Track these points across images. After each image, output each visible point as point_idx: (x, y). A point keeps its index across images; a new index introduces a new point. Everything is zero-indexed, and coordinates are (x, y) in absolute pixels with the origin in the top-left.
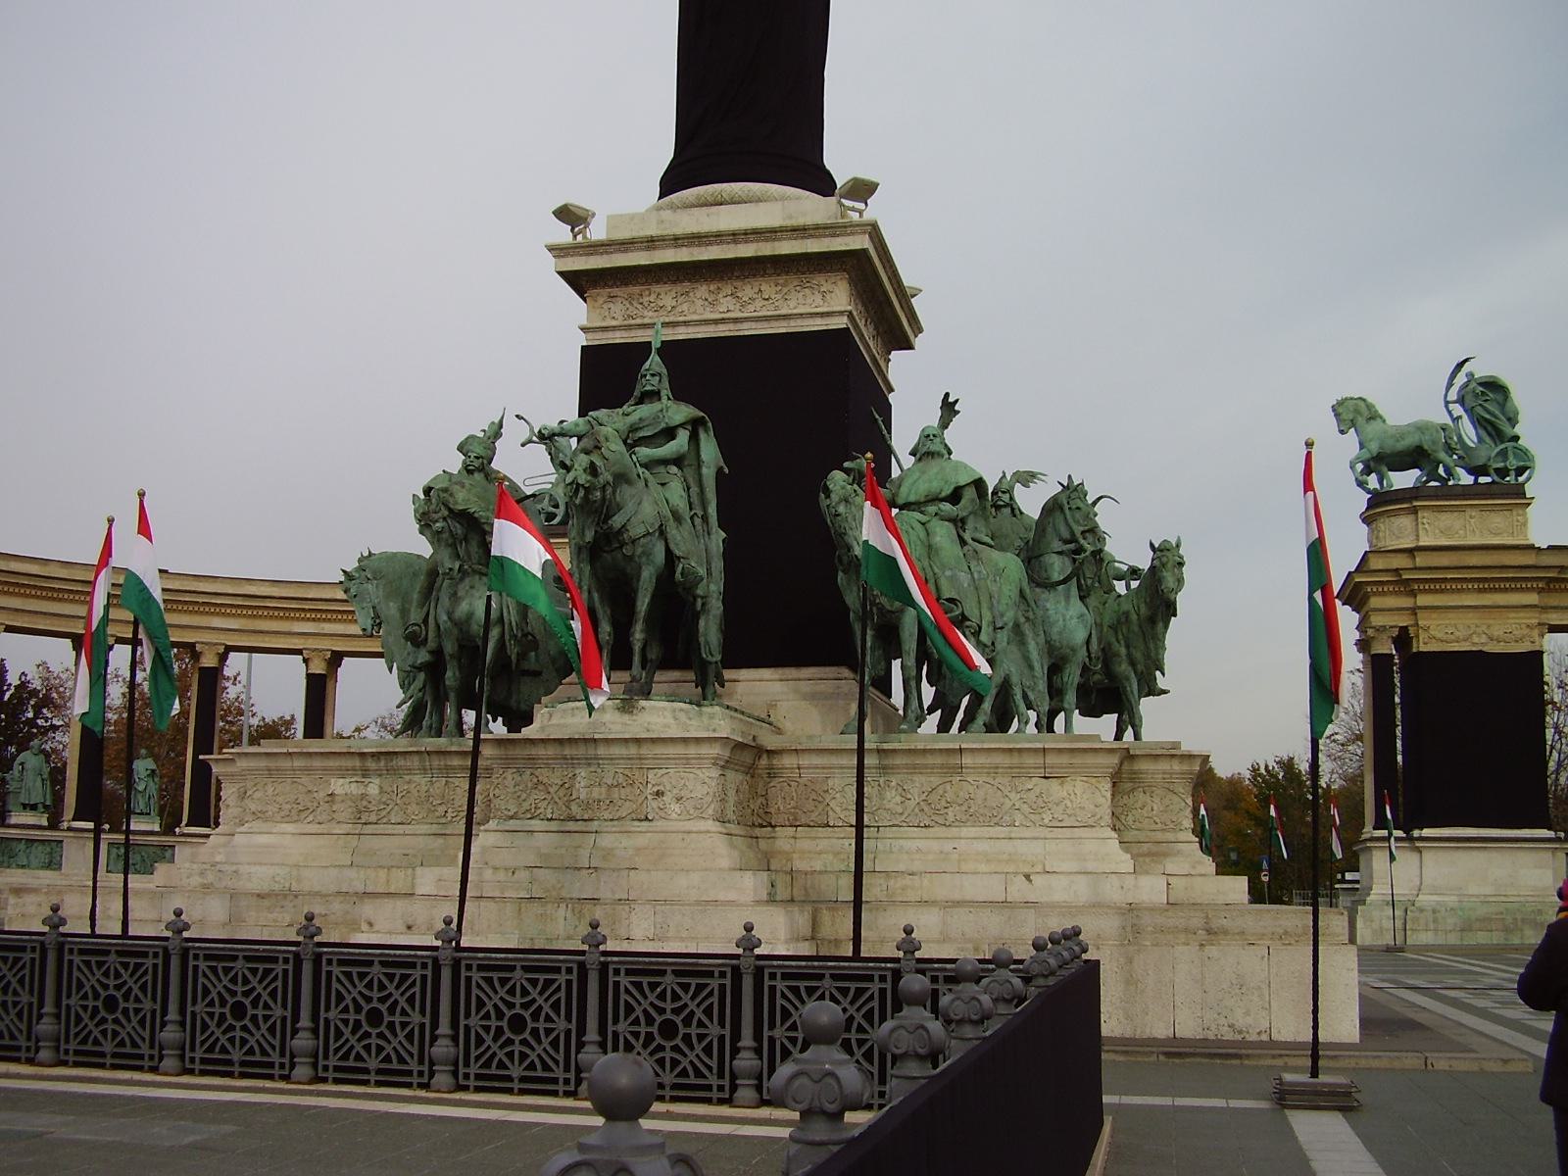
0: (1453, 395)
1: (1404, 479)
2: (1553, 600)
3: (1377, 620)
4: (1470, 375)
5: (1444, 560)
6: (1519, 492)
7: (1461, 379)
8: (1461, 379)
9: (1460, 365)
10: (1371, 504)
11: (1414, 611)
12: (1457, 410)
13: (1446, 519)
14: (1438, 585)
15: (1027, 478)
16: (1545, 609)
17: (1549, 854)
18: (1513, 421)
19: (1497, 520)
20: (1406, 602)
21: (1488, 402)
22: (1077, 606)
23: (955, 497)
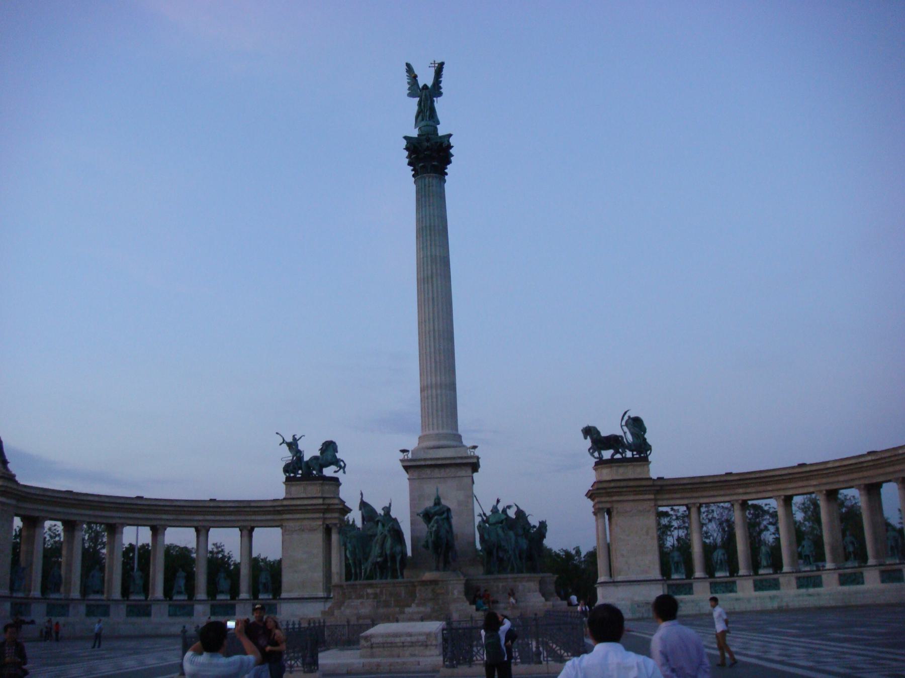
0: (624, 423)
1: (607, 454)
2: (658, 497)
3: (601, 506)
4: (629, 417)
5: (622, 484)
6: (645, 460)
7: (626, 418)
9: (625, 413)
10: (597, 464)
11: (610, 502)
12: (625, 429)
13: (621, 470)
14: (619, 493)
15: (509, 507)
16: (656, 500)
17: (661, 586)
18: (645, 432)
19: (639, 470)
20: (608, 499)
21: (636, 424)
22: (525, 541)
23: (501, 522)
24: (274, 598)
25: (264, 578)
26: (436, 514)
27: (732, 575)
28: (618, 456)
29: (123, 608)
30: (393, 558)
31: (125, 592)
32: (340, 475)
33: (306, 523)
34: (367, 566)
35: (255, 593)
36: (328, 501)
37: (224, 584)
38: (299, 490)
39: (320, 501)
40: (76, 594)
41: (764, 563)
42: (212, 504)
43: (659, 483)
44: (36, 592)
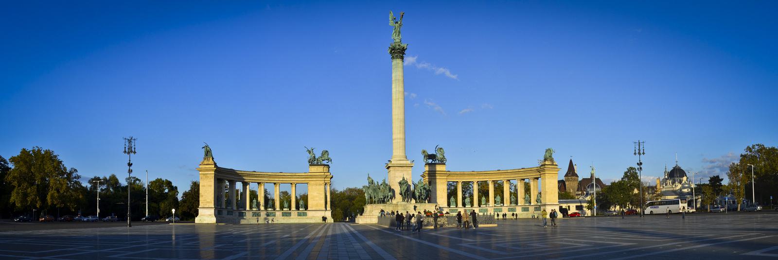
8: (437, 148)
24: (306, 210)
25: (301, 202)
26: (403, 184)
27: (471, 207)
28: (433, 162)
29: (251, 213)
30: (388, 197)
31: (251, 207)
32: (329, 164)
33: (318, 182)
34: (376, 199)
35: (297, 208)
36: (326, 174)
37: (286, 205)
38: (314, 169)
39: (323, 174)
40: (235, 208)
41: (483, 203)
42: (281, 174)
43: (448, 173)
44: (224, 207)
